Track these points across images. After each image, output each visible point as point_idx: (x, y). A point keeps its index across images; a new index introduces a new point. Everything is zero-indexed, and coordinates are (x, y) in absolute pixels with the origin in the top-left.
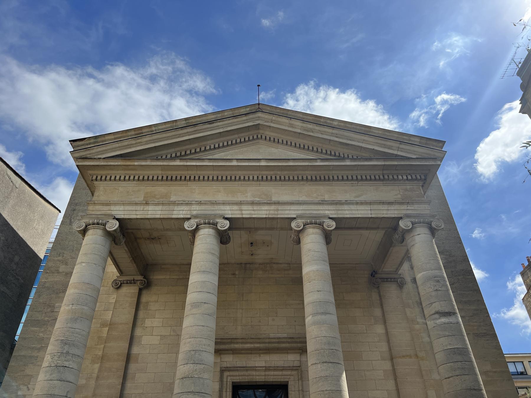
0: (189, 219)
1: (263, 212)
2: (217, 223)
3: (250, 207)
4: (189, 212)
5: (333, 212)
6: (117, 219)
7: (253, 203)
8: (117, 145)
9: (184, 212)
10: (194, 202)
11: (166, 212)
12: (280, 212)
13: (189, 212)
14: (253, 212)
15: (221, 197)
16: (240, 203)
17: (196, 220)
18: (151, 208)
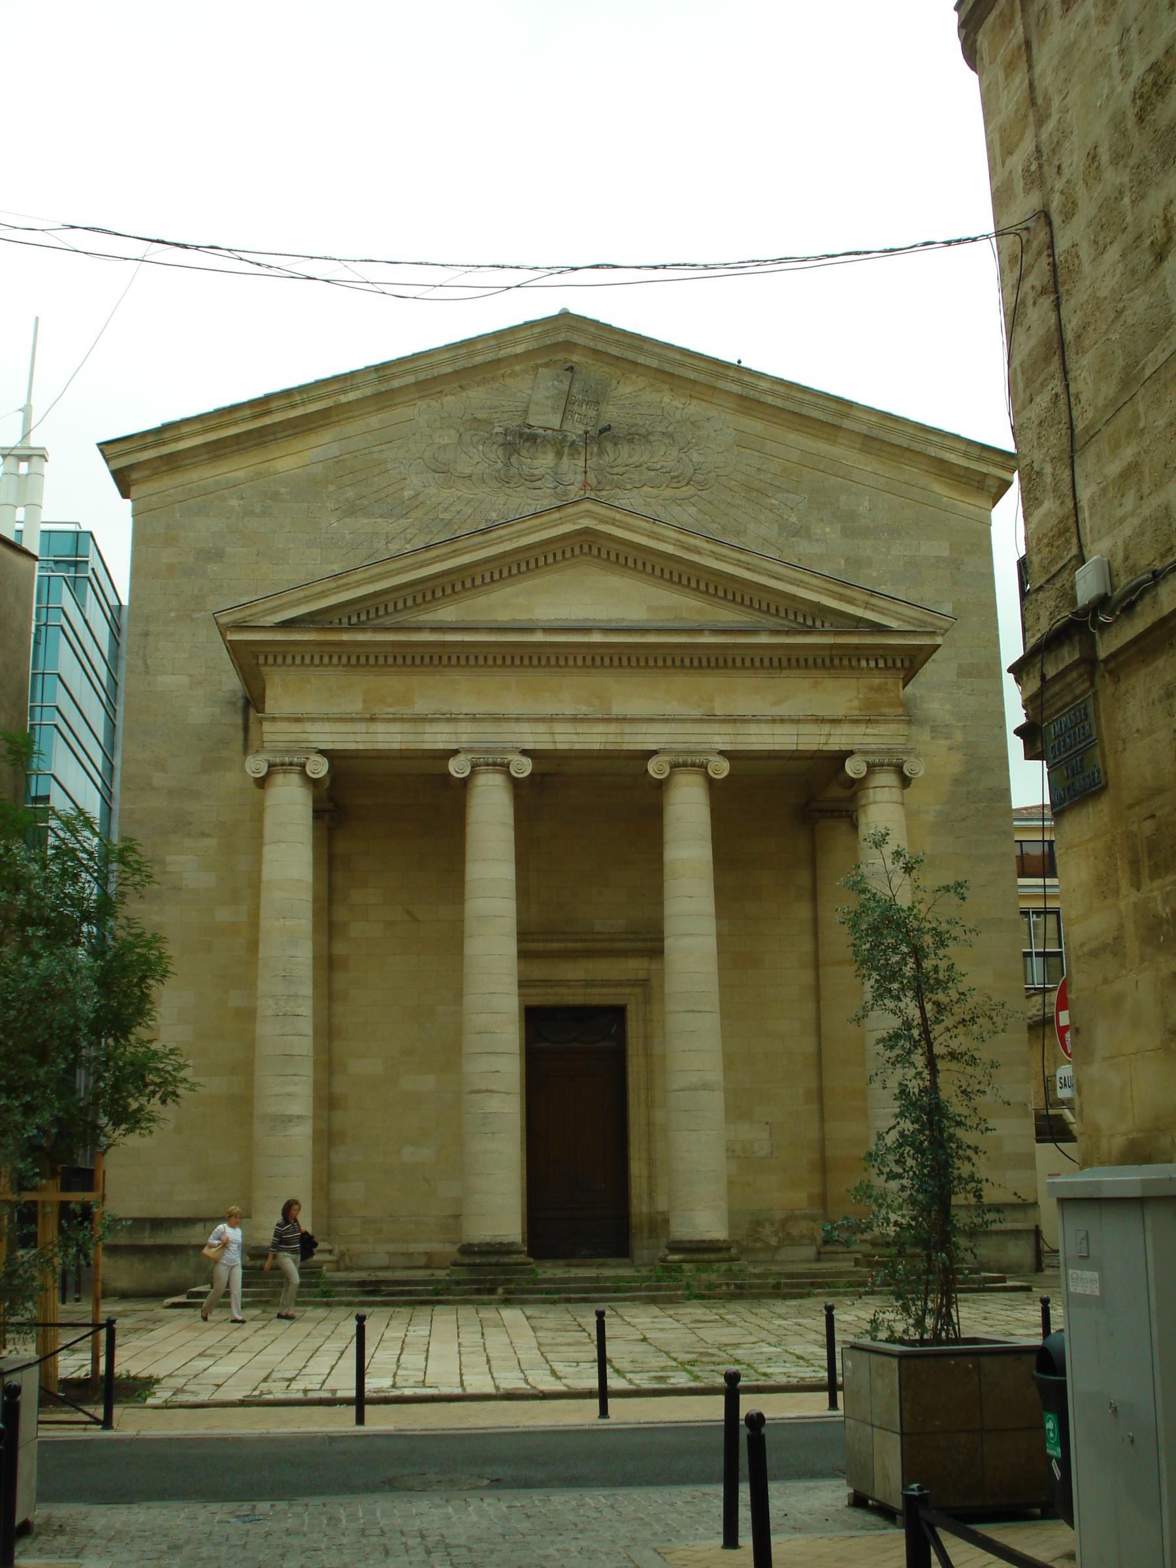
0: (456, 752)
1: (595, 738)
2: (509, 764)
3: (569, 728)
4: (453, 738)
5: (728, 739)
6: (322, 752)
7: (575, 719)
8: (301, 594)
9: (444, 737)
10: (462, 716)
11: (411, 738)
12: (627, 738)
13: (453, 738)
14: (575, 738)
15: (513, 705)
16: (551, 719)
17: (470, 756)
18: (380, 727)
